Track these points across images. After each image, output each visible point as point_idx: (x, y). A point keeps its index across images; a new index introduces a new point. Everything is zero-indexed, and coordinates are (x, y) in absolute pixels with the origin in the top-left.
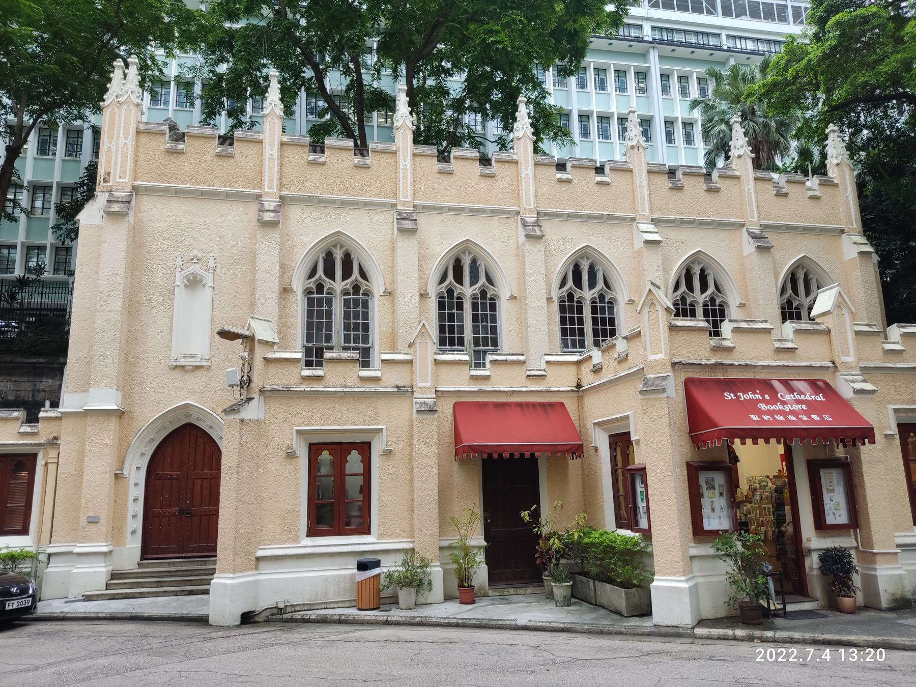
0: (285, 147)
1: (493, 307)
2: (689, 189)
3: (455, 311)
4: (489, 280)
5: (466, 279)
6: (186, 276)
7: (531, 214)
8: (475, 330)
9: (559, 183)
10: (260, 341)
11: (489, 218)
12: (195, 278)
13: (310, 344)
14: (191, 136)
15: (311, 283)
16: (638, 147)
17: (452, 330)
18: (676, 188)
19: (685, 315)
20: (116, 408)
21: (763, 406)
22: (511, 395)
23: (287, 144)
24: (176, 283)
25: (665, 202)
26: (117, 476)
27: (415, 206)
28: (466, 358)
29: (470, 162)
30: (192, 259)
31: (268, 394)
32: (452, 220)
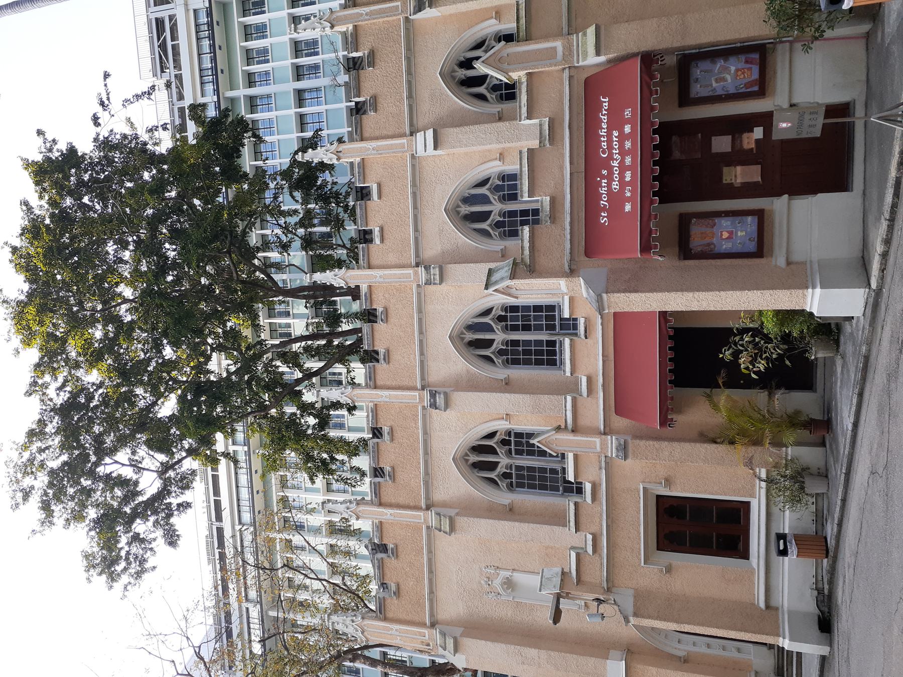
0: (383, 501)
1: (514, 309)
2: (374, 89)
3: (520, 349)
4: (487, 312)
5: (488, 336)
6: (504, 590)
7: (418, 273)
8: (539, 328)
9: (385, 241)
10: (561, 588)
11: (427, 315)
12: (505, 583)
13: (561, 488)
14: (383, 578)
15: (503, 484)
16: (337, 152)
17: (539, 353)
18: (374, 102)
19: (515, 187)
20: (624, 662)
21: (615, 185)
22: (607, 356)
23: (380, 500)
24: (511, 599)
25: (391, 119)
26: (686, 661)
27: (423, 388)
28: (567, 341)
29: (375, 333)
30: (489, 585)
31: (610, 585)
32: (431, 352)
